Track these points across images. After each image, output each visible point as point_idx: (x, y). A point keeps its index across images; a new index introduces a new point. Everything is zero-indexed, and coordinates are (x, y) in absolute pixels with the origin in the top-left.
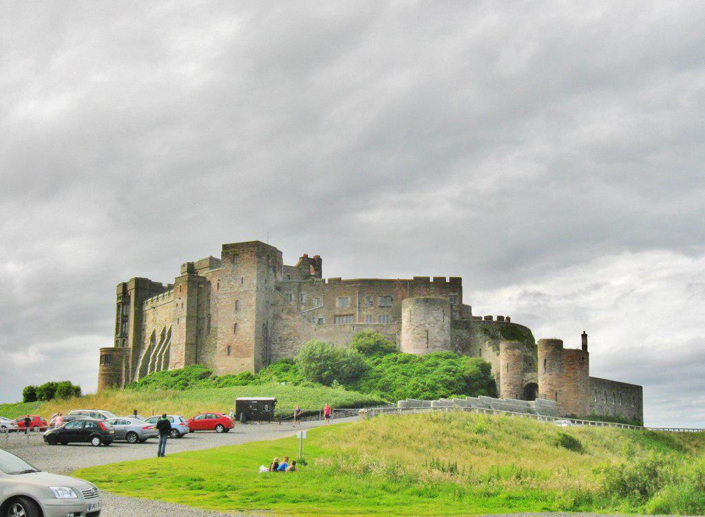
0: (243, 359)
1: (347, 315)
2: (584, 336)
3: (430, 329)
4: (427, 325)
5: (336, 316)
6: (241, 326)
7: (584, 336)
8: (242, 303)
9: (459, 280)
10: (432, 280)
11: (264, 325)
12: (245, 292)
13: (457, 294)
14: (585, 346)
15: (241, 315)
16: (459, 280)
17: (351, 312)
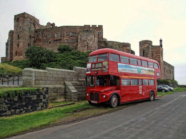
0: (20, 56)
1: (59, 40)
2: (161, 41)
3: (89, 42)
4: (87, 41)
5: (55, 40)
6: (20, 44)
7: (161, 41)
8: (20, 36)
9: (102, 26)
10: (91, 26)
11: (29, 44)
12: (21, 32)
13: (101, 31)
14: (161, 46)
15: (20, 40)
16: (102, 26)
17: (60, 38)
